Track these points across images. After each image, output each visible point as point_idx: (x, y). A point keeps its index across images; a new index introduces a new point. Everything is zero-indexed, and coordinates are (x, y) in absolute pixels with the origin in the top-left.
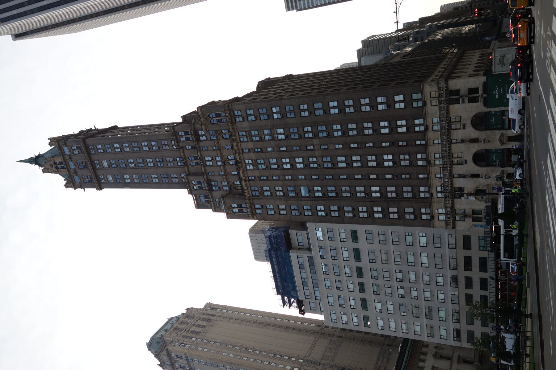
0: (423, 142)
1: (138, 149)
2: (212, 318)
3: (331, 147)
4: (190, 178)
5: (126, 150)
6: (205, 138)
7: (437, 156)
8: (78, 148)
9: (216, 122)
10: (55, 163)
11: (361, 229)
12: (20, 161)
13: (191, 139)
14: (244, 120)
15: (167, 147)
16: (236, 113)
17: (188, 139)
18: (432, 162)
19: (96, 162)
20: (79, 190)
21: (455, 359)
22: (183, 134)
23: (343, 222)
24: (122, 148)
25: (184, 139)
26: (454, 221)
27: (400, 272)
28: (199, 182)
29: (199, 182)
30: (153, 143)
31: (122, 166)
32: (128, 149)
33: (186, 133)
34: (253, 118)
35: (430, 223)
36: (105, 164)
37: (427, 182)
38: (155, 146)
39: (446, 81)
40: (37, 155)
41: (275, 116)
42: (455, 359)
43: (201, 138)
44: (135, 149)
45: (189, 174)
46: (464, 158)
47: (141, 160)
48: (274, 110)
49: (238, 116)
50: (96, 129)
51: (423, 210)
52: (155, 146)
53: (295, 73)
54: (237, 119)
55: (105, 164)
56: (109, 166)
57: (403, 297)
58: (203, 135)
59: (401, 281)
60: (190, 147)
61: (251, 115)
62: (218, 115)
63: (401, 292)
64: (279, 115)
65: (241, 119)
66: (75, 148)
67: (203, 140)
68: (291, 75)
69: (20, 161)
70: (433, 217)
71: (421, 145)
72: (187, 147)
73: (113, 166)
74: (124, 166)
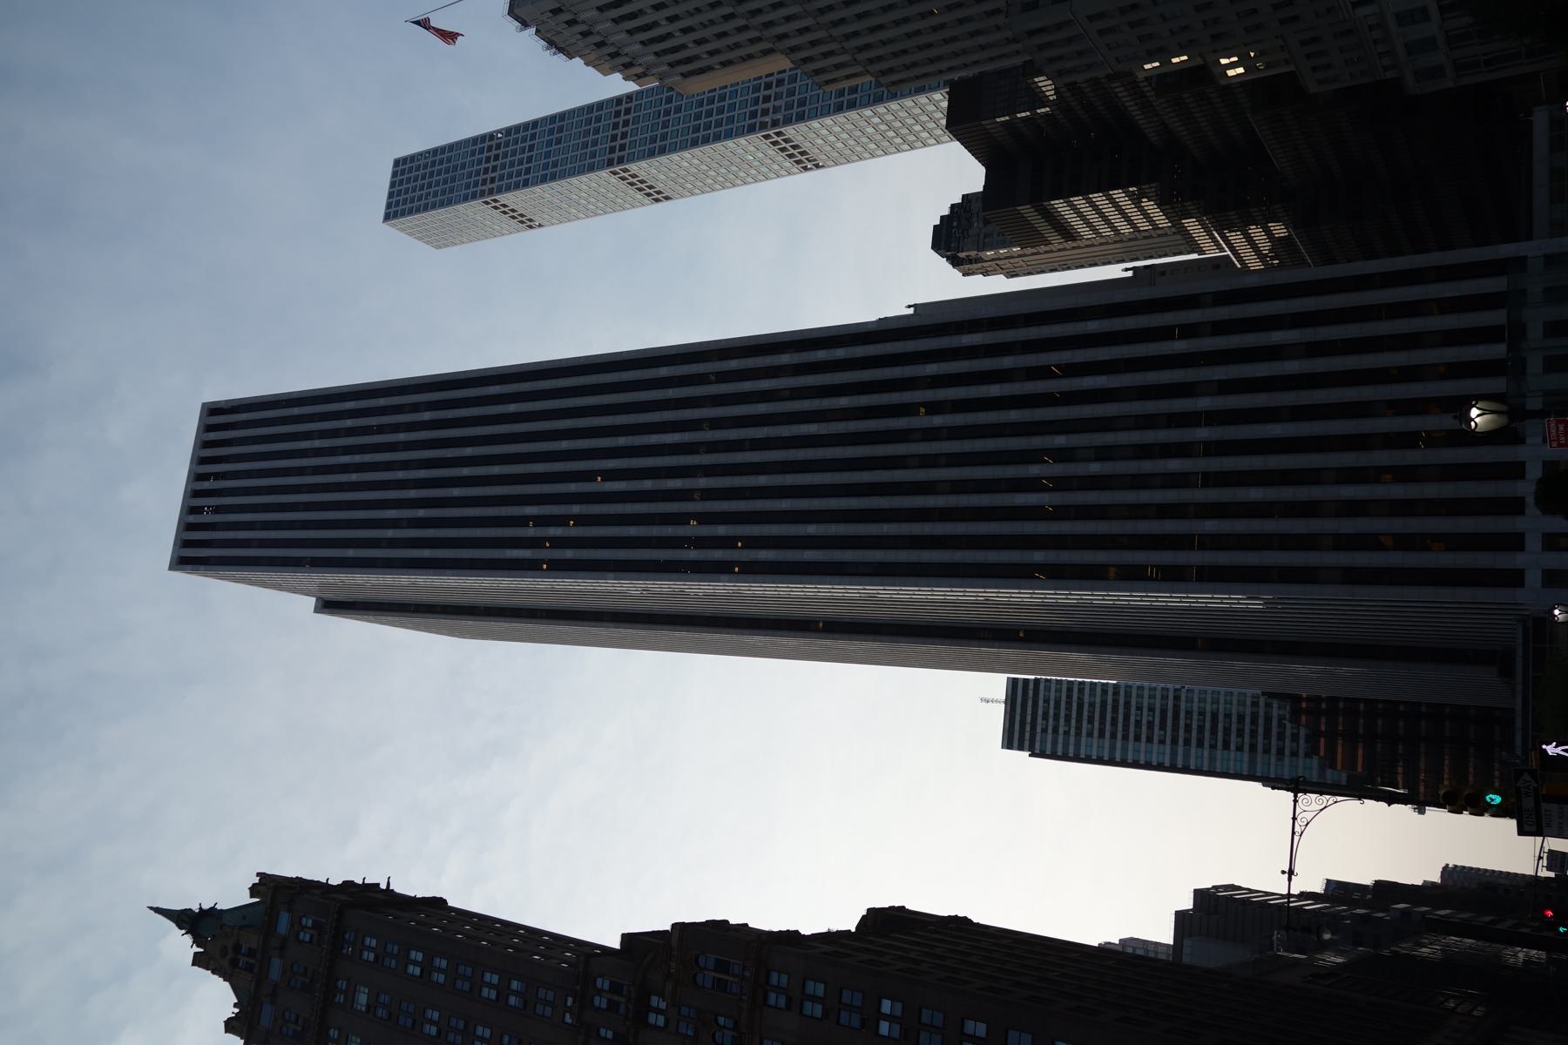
1: (467, 986)
5: (435, 976)
6: (661, 1021)
8: (316, 925)
9: (709, 984)
10: (237, 948)
12: (158, 910)
13: (622, 1007)
14: (788, 1008)
15: (548, 1011)
16: (774, 977)
17: (613, 1006)
19: (342, 984)
22: (606, 986)
24: (427, 967)
25: (604, 1006)
30: (515, 985)
31: (402, 1021)
32: (441, 978)
33: (615, 988)
34: (818, 1011)
36: (363, 999)
38: (516, 993)
40: (206, 907)
41: (884, 1028)
43: (652, 1018)
44: (459, 984)
47: (461, 1024)
48: (886, 1006)
49: (778, 989)
50: (389, 891)
52: (516, 993)
53: (976, 918)
54: (772, 997)
55: (363, 999)
56: (368, 1006)
58: (658, 1011)
60: (610, 1035)
61: (814, 999)
62: (722, 966)
64: (897, 1027)
65: (782, 1002)
66: (310, 923)
67: (655, 1027)
68: (966, 920)
69: (158, 910)
72: (603, 1032)
73: (380, 1012)
74: (409, 1023)
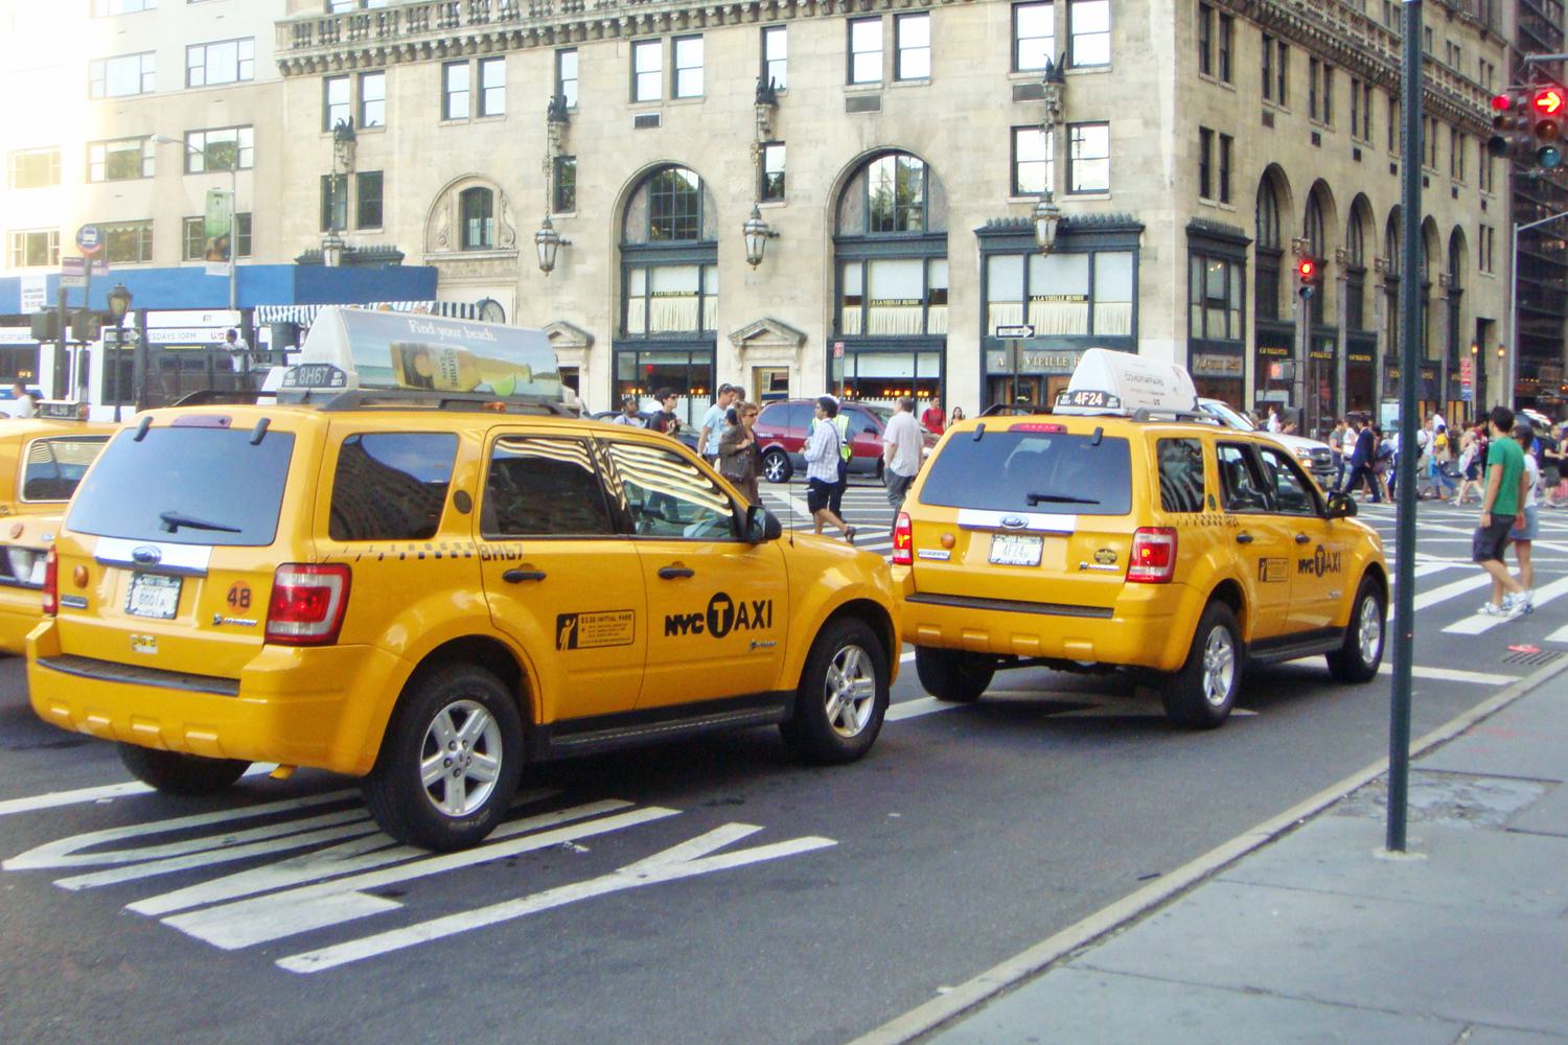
46: (672, 116)
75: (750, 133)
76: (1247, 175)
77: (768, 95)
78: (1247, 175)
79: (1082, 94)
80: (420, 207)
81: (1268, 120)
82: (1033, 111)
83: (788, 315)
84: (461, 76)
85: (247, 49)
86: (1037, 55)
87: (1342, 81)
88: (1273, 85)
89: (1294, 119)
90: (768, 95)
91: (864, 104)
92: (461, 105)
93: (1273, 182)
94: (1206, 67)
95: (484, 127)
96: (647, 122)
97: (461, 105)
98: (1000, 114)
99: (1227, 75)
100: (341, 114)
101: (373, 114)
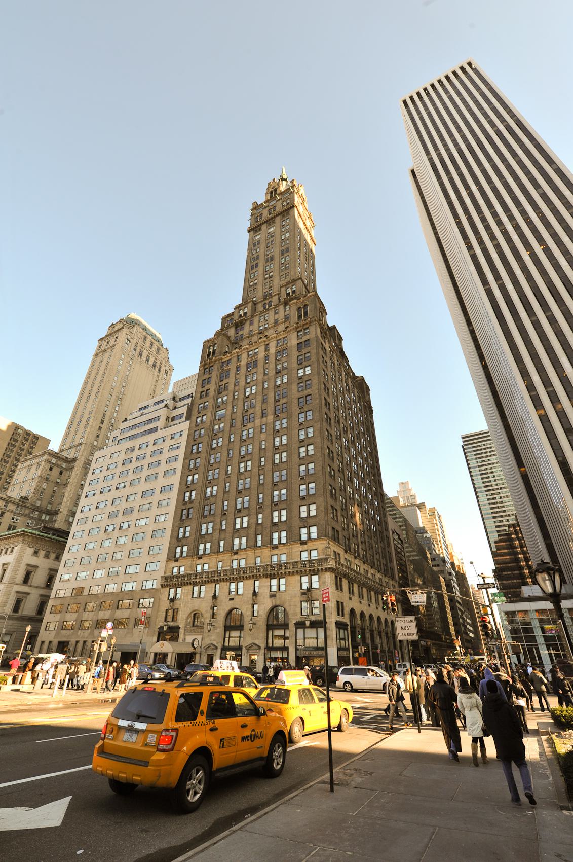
0: (259, 544)
2: (157, 369)
3: (263, 436)
4: (250, 305)
7: (243, 562)
11: (175, 480)
18: (236, 557)
20: (250, 213)
21: (25, 589)
23: (185, 458)
26: (169, 586)
27: (129, 526)
28: (245, 314)
29: (245, 314)
35: (172, 557)
37: (216, 551)
39: (331, 570)
42: (25, 589)
45: (255, 304)
46: (237, 598)
51: (185, 548)
57: (106, 531)
59: (120, 528)
63: (110, 529)
70: (176, 561)
71: (256, 541)
75: (251, 602)
76: (347, 610)
77: (255, 594)
78: (347, 610)
79: (315, 594)
80: (185, 617)
81: (350, 599)
82: (304, 598)
83: (257, 642)
84: (196, 588)
85: (155, 582)
86: (305, 586)
87: (365, 590)
88: (351, 592)
89: (356, 598)
90: (255, 594)
91: (273, 596)
92: (195, 595)
93: (352, 611)
94: (337, 588)
95: (200, 600)
96: (231, 599)
97: (195, 595)
98: (298, 599)
99: (341, 590)
100: (172, 596)
101: (178, 596)
